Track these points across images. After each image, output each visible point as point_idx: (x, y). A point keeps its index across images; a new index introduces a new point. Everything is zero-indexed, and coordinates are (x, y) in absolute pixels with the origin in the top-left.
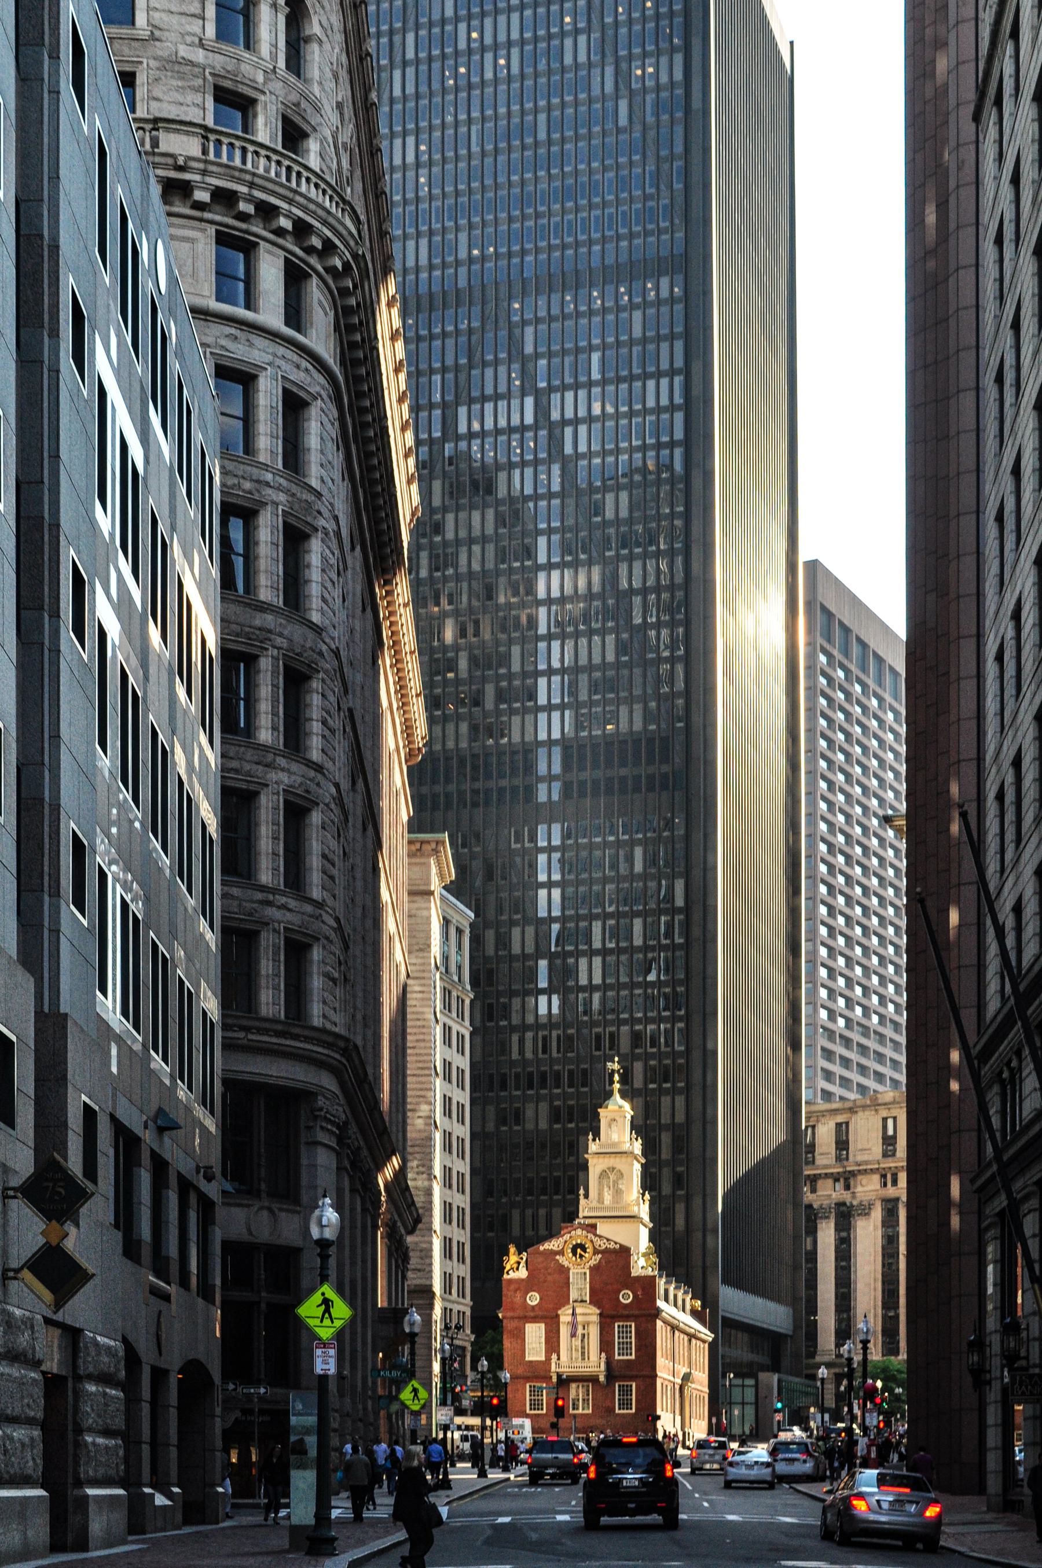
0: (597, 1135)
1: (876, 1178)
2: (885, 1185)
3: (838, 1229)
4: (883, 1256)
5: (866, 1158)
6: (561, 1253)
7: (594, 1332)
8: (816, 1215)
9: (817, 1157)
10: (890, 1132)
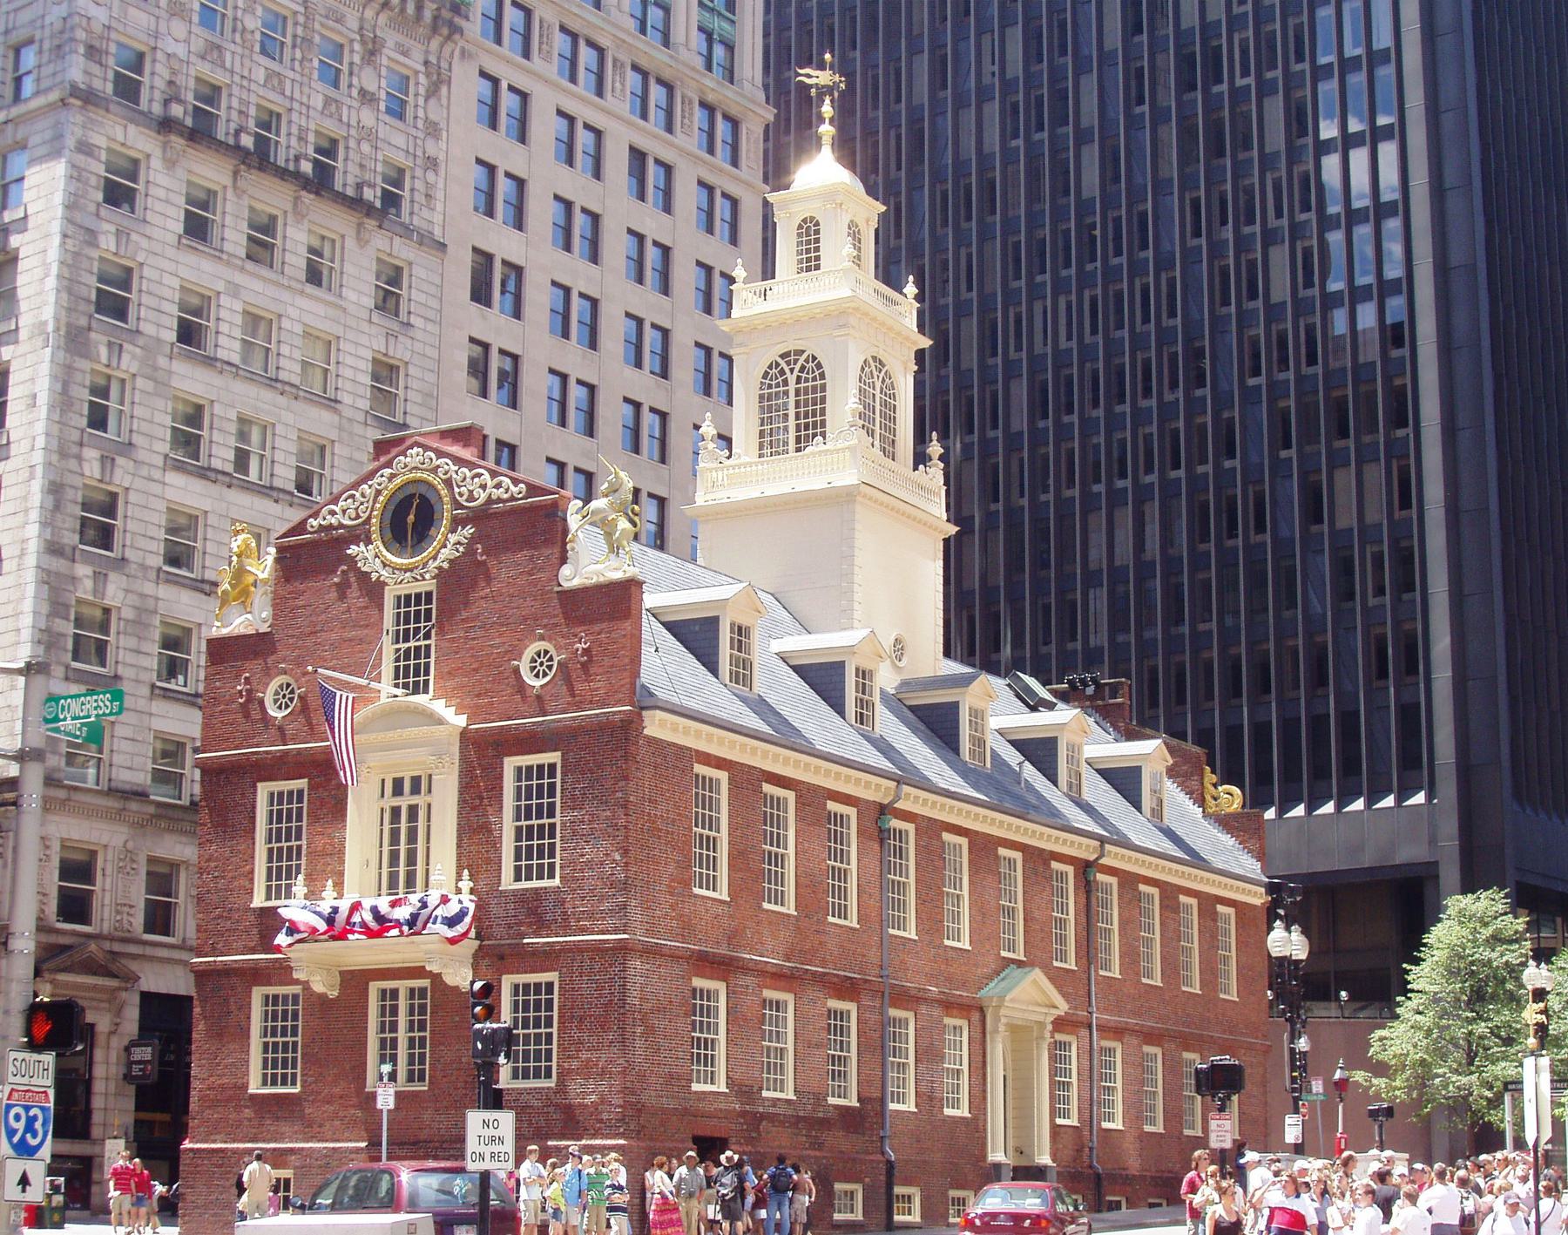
6: (359, 534)
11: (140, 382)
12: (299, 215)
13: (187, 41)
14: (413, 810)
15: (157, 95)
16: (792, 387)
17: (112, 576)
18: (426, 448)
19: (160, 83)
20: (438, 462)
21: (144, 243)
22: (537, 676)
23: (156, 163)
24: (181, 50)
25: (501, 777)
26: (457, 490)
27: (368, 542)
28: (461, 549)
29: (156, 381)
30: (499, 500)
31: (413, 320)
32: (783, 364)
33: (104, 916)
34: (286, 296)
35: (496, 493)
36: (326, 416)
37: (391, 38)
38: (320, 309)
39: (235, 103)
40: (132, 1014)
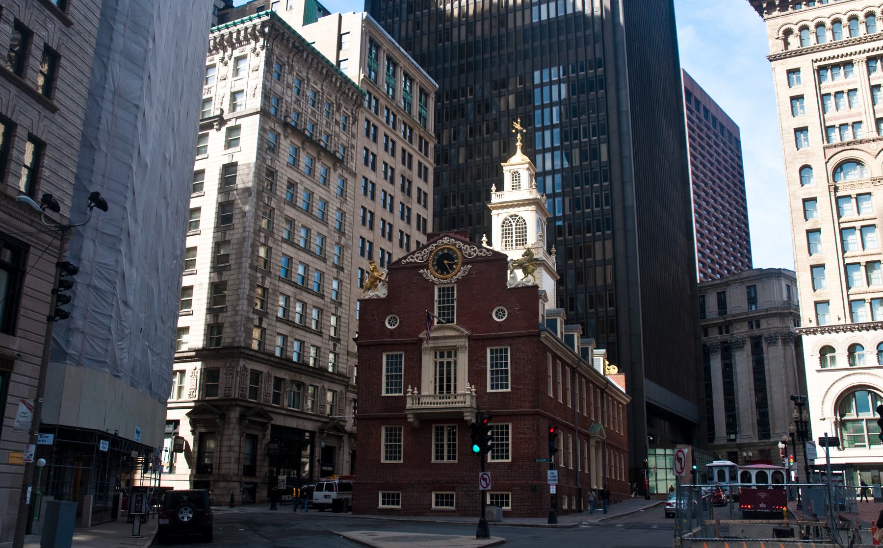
0: (500, 188)
1: (746, 324)
2: (752, 327)
3: (723, 358)
4: (754, 373)
5: (738, 312)
6: (425, 266)
7: (463, 360)
8: (708, 350)
9: (707, 314)
10: (753, 295)
11: (276, 211)
12: (319, 160)
13: (291, 97)
14: (449, 363)
15: (283, 114)
16: (514, 227)
17: (267, 278)
18: (451, 237)
19: (283, 110)
21: (278, 163)
22: (499, 318)
23: (282, 137)
24: (289, 99)
25: (486, 353)
27: (428, 269)
29: (281, 212)
30: (481, 256)
31: (348, 198)
32: (510, 219)
33: (262, 398)
34: (315, 186)
36: (325, 228)
37: (344, 105)
38: (323, 191)
39: (303, 120)
40: (269, 432)
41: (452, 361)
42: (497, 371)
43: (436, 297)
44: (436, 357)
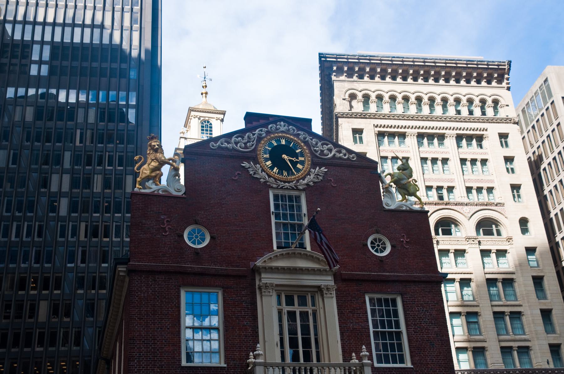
14: (305, 315)
18: (289, 124)
20: (300, 132)
26: (312, 148)
28: (321, 178)
30: (340, 158)
35: (338, 155)
41: (310, 312)
42: (383, 333)
43: (272, 209)
44: (279, 303)
